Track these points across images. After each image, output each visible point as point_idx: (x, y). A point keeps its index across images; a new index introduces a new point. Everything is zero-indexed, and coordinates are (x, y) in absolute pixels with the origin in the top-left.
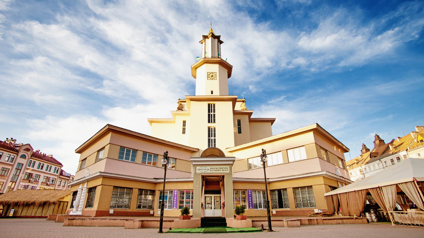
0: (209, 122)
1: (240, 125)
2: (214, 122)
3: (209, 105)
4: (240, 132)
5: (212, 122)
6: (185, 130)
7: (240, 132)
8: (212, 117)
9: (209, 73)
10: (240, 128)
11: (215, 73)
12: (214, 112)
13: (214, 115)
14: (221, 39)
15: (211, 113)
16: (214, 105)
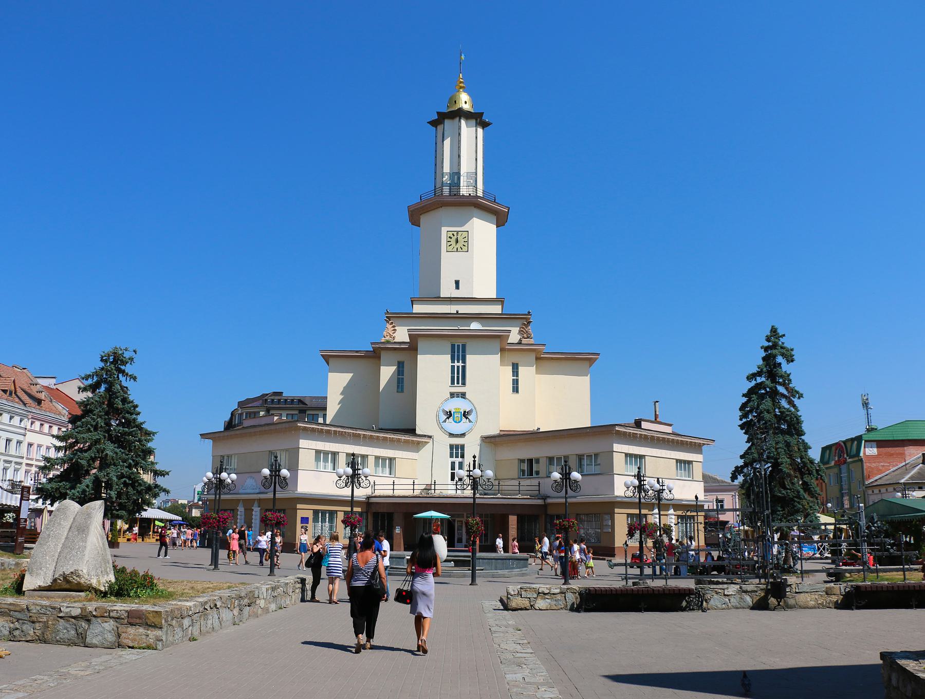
0: (453, 383)
1: (517, 376)
2: (464, 384)
3: (453, 346)
4: (516, 389)
5: (458, 383)
6: (403, 382)
7: (516, 389)
8: (458, 373)
9: (450, 234)
10: (517, 380)
11: (465, 234)
12: (464, 361)
13: (464, 368)
14: (486, 118)
15: (456, 364)
16: (464, 346)
